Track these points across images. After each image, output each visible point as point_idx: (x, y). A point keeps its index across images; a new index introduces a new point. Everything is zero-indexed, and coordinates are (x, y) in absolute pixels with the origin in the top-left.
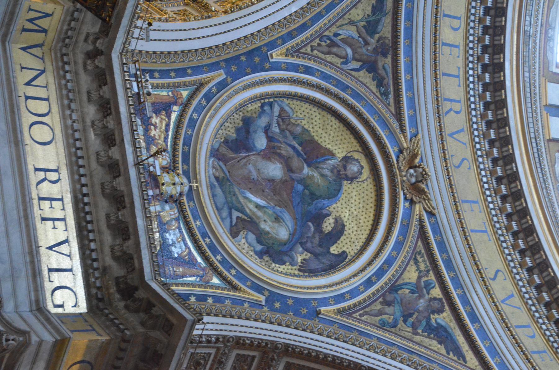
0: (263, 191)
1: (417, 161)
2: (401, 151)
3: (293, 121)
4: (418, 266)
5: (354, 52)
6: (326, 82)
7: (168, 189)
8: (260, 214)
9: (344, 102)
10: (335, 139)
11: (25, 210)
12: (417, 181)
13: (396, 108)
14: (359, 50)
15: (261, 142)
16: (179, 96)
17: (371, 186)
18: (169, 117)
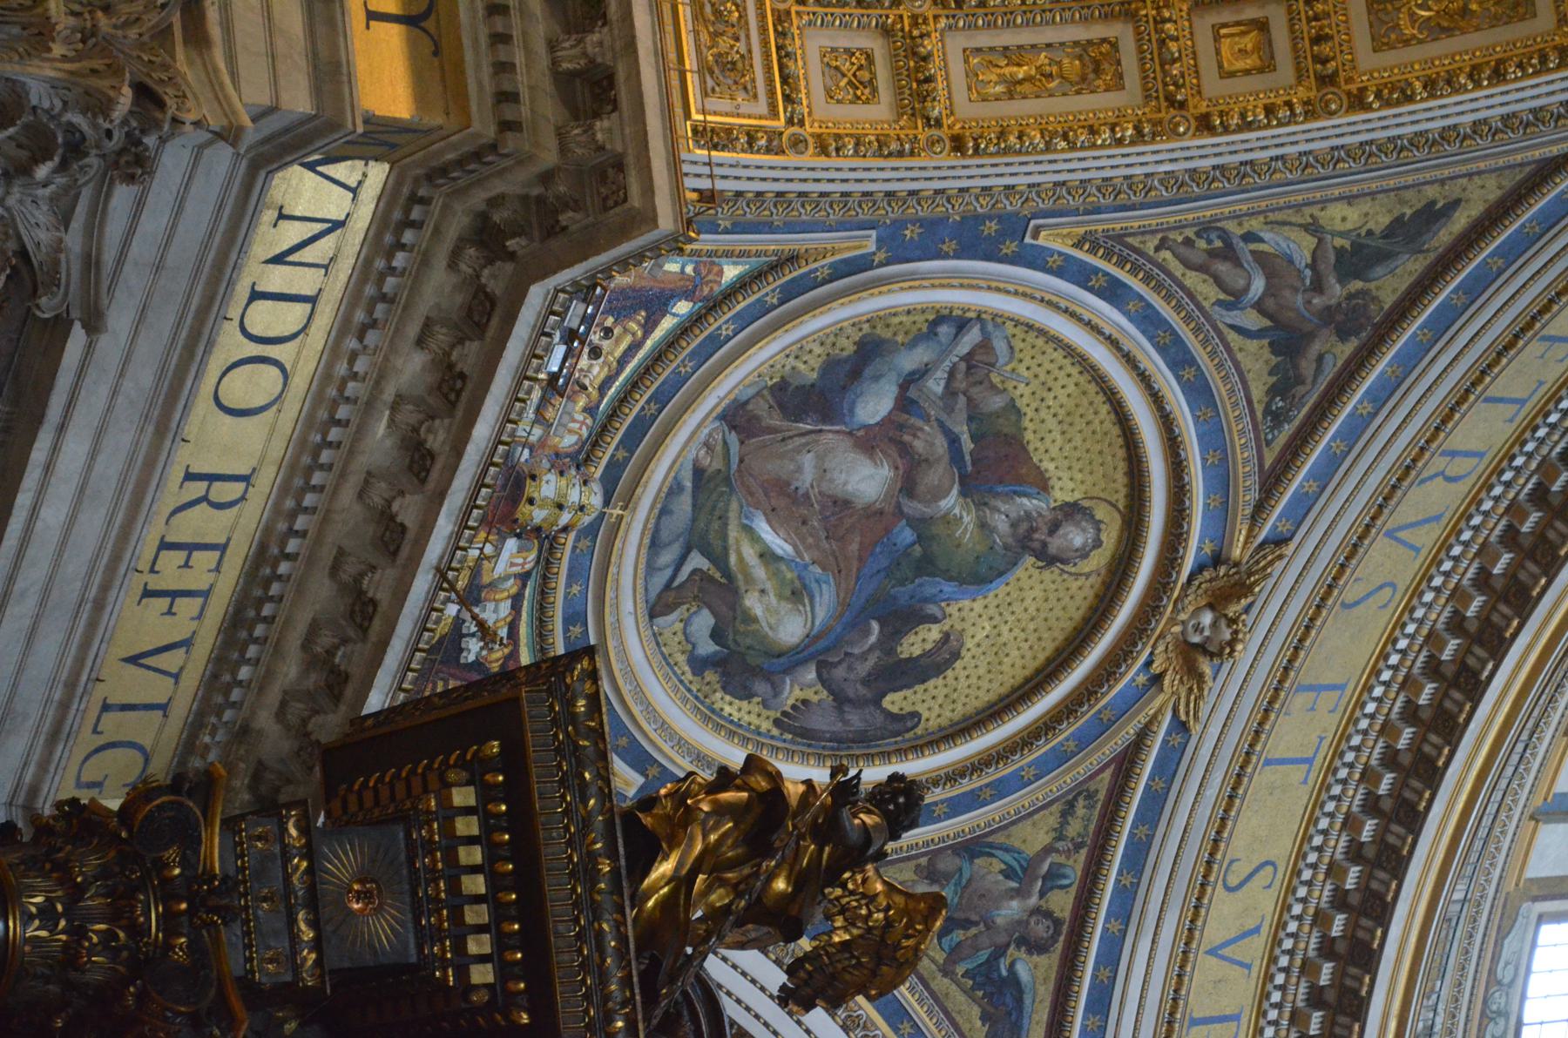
0: (804, 523)
1: (1232, 610)
2: (1217, 559)
3: (995, 379)
4: (1064, 823)
5: (1270, 291)
6: (1144, 332)
7: (538, 515)
8: (760, 572)
9: (1156, 399)
10: (1077, 454)
11: (105, 588)
12: (1202, 648)
13: (1278, 461)
14: (1287, 293)
15: (875, 405)
16: (710, 277)
17: (1090, 594)
18: (649, 327)
